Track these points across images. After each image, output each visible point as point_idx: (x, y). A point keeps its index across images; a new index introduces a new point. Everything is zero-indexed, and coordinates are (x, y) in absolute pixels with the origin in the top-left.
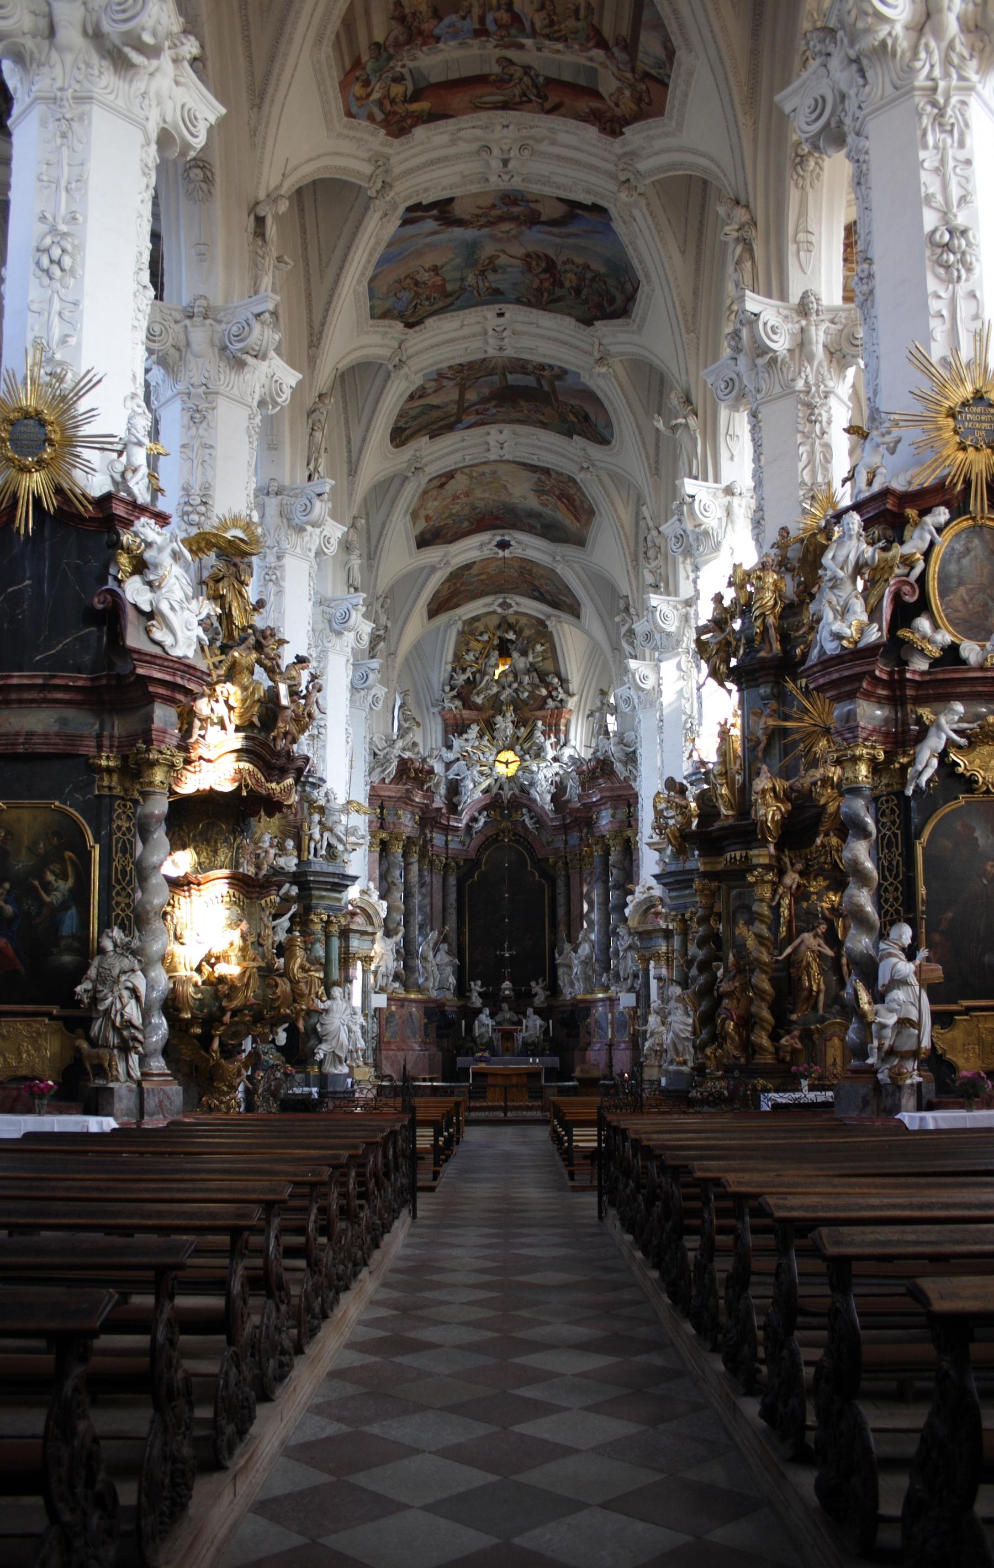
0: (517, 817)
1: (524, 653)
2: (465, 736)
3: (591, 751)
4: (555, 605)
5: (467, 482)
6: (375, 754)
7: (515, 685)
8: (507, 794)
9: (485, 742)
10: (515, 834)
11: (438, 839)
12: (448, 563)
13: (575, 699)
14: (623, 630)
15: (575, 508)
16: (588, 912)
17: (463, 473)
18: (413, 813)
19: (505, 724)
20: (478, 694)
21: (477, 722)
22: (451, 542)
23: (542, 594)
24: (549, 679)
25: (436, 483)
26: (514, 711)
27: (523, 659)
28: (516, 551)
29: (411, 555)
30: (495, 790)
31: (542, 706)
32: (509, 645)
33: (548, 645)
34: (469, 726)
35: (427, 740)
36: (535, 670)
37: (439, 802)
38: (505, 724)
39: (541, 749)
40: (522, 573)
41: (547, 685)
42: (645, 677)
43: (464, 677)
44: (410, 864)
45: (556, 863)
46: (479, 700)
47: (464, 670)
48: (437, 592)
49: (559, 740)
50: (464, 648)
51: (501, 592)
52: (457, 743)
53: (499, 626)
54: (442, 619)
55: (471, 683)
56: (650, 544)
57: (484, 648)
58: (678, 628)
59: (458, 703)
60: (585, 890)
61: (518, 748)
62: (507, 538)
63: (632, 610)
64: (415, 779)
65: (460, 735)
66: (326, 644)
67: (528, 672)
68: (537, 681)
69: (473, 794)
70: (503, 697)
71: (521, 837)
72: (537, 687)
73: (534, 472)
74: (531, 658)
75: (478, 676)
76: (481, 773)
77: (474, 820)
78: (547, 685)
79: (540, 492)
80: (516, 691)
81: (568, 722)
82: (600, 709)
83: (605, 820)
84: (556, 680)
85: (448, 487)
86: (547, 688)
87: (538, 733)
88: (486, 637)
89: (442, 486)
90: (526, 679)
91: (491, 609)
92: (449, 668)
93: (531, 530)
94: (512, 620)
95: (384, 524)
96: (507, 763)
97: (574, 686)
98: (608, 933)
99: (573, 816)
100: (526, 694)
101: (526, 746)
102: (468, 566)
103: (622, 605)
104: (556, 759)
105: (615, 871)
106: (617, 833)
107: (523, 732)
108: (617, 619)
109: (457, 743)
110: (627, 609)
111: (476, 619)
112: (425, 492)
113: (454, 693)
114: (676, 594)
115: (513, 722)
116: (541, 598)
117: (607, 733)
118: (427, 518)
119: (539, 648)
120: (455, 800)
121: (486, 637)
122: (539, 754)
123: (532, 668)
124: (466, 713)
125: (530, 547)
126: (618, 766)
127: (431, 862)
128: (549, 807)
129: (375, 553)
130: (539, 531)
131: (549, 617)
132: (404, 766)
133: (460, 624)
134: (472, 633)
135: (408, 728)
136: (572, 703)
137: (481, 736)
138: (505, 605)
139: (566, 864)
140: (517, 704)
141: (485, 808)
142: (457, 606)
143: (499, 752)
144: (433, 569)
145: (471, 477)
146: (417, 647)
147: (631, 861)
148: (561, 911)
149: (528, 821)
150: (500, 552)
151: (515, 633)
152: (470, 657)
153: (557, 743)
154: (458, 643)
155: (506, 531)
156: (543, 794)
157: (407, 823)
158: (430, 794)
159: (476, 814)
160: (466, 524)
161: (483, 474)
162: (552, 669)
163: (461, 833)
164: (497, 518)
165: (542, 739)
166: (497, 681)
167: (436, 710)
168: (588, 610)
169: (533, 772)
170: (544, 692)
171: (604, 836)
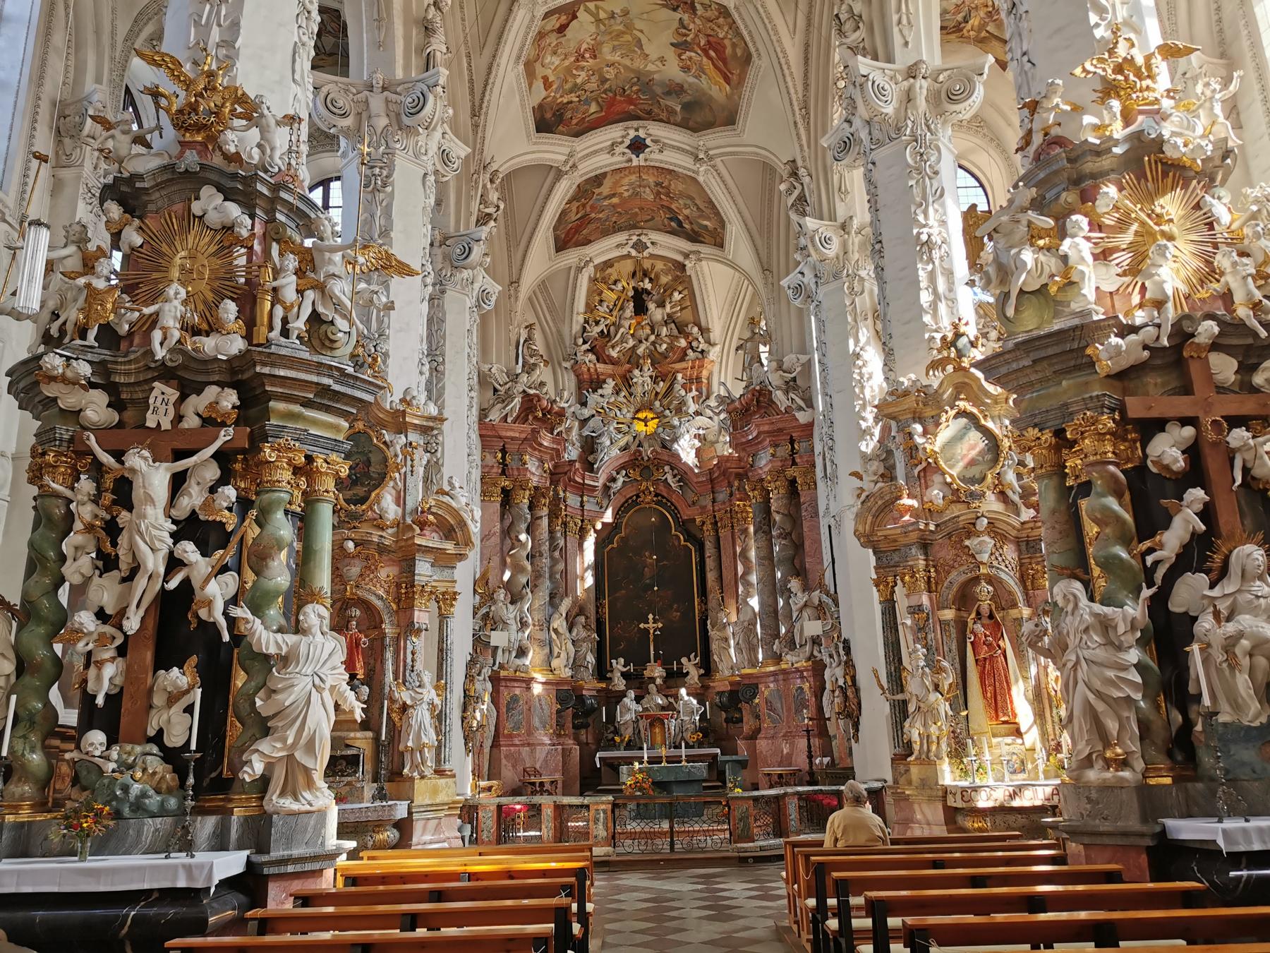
0: (657, 476)
1: (661, 305)
2: (600, 391)
3: (744, 384)
4: (694, 237)
5: (593, 29)
6: (495, 390)
7: (652, 338)
8: (647, 451)
10: (657, 495)
11: (573, 500)
12: (574, 166)
13: (718, 348)
14: (791, 200)
15: (724, 61)
16: (745, 574)
17: (587, 10)
18: (542, 461)
19: (642, 378)
20: (613, 347)
21: (613, 377)
22: (577, 134)
23: (680, 224)
24: (688, 329)
25: (554, 23)
27: (660, 311)
28: (653, 156)
29: (528, 136)
30: (633, 448)
32: (645, 297)
33: (686, 292)
34: (604, 382)
35: (557, 386)
37: (572, 453)
38: (642, 378)
39: (683, 403)
40: (658, 193)
41: (687, 336)
42: (827, 240)
43: (598, 329)
46: (614, 354)
47: (597, 323)
48: (564, 213)
49: (701, 393)
50: (597, 298)
51: (635, 227)
52: (593, 398)
53: (634, 274)
54: (572, 257)
56: (843, 17)
57: (619, 298)
58: (897, 110)
59: (591, 357)
60: (738, 550)
61: (657, 403)
62: (642, 134)
63: (802, 172)
64: (543, 420)
65: (595, 391)
66: (391, 144)
68: (675, 332)
69: (611, 453)
70: (640, 351)
71: (661, 499)
73: (675, 10)
74: (668, 309)
75: (612, 329)
76: (619, 431)
77: (614, 480)
78: (687, 336)
79: (681, 46)
80: (653, 343)
81: (711, 374)
82: (750, 339)
83: (764, 462)
84: (696, 329)
85: (569, 32)
86: (686, 337)
87: (677, 387)
88: (619, 287)
89: (562, 29)
90: (664, 331)
91: (625, 253)
92: (581, 319)
93: (668, 119)
94: (647, 265)
95: (490, 68)
96: (645, 421)
97: (716, 335)
98: (772, 590)
99: (720, 476)
100: (664, 346)
101: (665, 402)
102: (598, 180)
103: (784, 171)
104: (698, 413)
105: (777, 518)
106: (778, 473)
108: (783, 187)
109: (593, 398)
110: (794, 174)
111: (608, 264)
112: (541, 35)
113: (587, 346)
114: (890, 59)
115: (651, 377)
116: (678, 228)
117: (762, 365)
118: (547, 84)
119: (677, 296)
122: (679, 411)
123: (670, 319)
125: (670, 146)
126: (779, 396)
127: (565, 524)
129: (481, 108)
130: (679, 118)
131: (686, 256)
132: (530, 404)
133: (591, 268)
134: (604, 281)
135: (535, 365)
136: (714, 353)
137: (617, 392)
138: (640, 246)
139: (716, 523)
140: (657, 359)
141: (623, 467)
142: (587, 242)
143: (637, 412)
144: (559, 174)
145: (598, 21)
146: (543, 285)
147: (798, 505)
148: (711, 576)
149: (670, 481)
150: (634, 157)
151: (651, 280)
152: (603, 309)
154: (590, 293)
155: (641, 123)
156: (686, 450)
157: (534, 471)
158: (561, 440)
159: (614, 473)
160: (594, 108)
161: (612, 16)
162: (691, 319)
164: (630, 101)
165: (683, 392)
166: (633, 335)
167: (567, 365)
168: (735, 232)
169: (674, 427)
171: (762, 480)
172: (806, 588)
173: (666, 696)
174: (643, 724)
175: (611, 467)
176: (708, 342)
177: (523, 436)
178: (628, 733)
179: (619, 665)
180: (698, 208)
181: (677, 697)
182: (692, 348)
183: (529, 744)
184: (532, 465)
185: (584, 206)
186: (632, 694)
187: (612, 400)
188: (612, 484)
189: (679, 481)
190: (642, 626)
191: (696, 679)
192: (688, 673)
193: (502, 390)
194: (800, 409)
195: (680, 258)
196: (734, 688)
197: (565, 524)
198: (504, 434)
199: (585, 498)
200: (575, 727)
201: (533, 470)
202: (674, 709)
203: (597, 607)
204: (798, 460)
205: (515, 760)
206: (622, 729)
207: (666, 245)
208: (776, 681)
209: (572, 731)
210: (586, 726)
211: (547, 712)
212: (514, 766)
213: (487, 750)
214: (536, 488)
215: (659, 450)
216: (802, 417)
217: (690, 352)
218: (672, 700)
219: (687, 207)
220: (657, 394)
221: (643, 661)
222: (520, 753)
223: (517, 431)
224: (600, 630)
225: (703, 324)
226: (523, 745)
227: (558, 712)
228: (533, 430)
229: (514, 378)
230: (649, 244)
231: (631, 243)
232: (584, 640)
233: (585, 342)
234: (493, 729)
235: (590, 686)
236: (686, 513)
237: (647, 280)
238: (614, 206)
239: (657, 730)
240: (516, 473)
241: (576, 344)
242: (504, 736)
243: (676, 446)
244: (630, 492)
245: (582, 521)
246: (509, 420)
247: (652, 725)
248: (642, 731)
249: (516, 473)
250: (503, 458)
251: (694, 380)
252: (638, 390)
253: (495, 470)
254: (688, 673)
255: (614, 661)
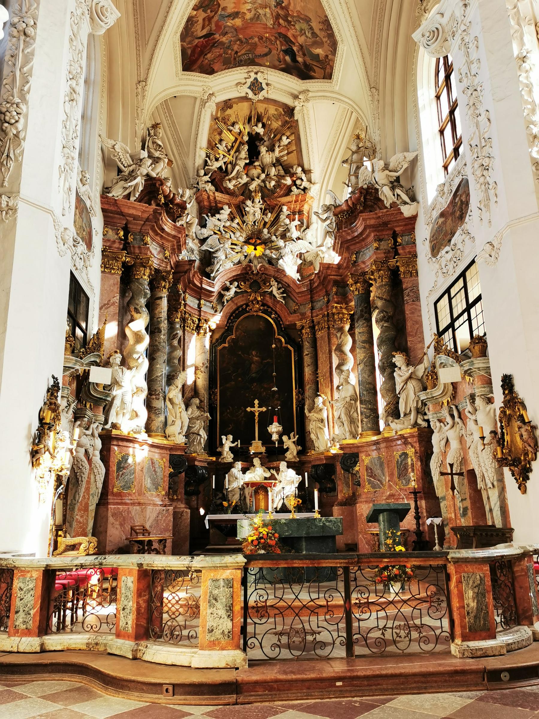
2: (218, 216)
4: (304, 73)
6: (120, 171)
9: (234, 225)
11: (192, 301)
19: (254, 209)
20: (230, 180)
26: (262, 198)
30: (244, 264)
31: (289, 191)
33: (293, 137)
36: (281, 165)
38: (254, 209)
39: (288, 230)
40: (278, 17)
41: (292, 175)
44: (161, 298)
45: (303, 327)
46: (231, 185)
49: (302, 223)
50: (218, 137)
52: (212, 221)
55: (223, 172)
61: (265, 231)
65: (213, 215)
67: (274, 165)
68: (282, 172)
69: (225, 266)
70: (252, 187)
72: (283, 177)
74: (277, 153)
75: (229, 166)
77: (227, 289)
80: (263, 181)
87: (282, 217)
88: (236, 129)
90: (273, 171)
91: (243, 95)
92: (204, 155)
94: (261, 108)
97: (314, 176)
100: (273, 183)
101: (273, 230)
104: (298, 239)
106: (381, 264)
107: (269, 217)
115: (261, 209)
119: (285, 141)
120: (208, 270)
121: (236, 129)
123: (278, 162)
124: (219, 196)
127: (184, 320)
128: (295, 276)
132: (153, 186)
134: (225, 120)
138: (256, 87)
148: (308, 371)
149: (275, 292)
151: (264, 126)
153: (301, 226)
154: (212, 131)
156: (290, 267)
159: (228, 283)
162: (296, 162)
163: (214, 299)
165: (287, 221)
170: (288, 181)
172: (409, 363)
173: (269, 469)
174: (248, 491)
175: (226, 278)
176: (310, 181)
177: (146, 215)
178: (235, 499)
179: (227, 442)
180: (314, 34)
181: (278, 470)
182: (296, 185)
183: (139, 504)
184: (154, 249)
185: (210, 19)
186: (239, 465)
187: (228, 224)
188: (226, 293)
189: (282, 293)
190: (249, 409)
191: (295, 453)
192: (287, 449)
193: (127, 171)
194: (405, 203)
195: (289, 101)
196: (328, 462)
197: (184, 320)
198: (126, 210)
199: (202, 302)
200: (187, 493)
201: (155, 252)
202: (276, 479)
203: (210, 394)
204: (400, 251)
205: (123, 519)
206: (230, 495)
207: (280, 85)
208: (378, 449)
209: (184, 497)
210: (196, 493)
211: (160, 474)
212: (121, 525)
213: (92, 508)
214: (157, 271)
215: (267, 266)
216: (407, 211)
217: (294, 188)
218: (274, 472)
219: (302, 32)
220: (265, 223)
221: (247, 441)
222: (129, 512)
223: (139, 210)
224: (212, 410)
225: (306, 167)
226: (133, 504)
227: (171, 475)
228: (155, 211)
229: (139, 162)
230: (264, 86)
231: (249, 81)
232: (197, 418)
233: (205, 174)
234: (100, 485)
235: (201, 457)
236: (289, 319)
237: (260, 125)
238: (236, 29)
239: (261, 497)
240: (137, 251)
241: (198, 175)
242: (113, 494)
243: (281, 261)
244: (241, 301)
245: (199, 320)
246: (132, 199)
247: (256, 492)
248: (248, 498)
249: (137, 251)
250: (126, 235)
251: (297, 213)
252: (250, 219)
253: (116, 245)
254: (287, 449)
255: (224, 437)
